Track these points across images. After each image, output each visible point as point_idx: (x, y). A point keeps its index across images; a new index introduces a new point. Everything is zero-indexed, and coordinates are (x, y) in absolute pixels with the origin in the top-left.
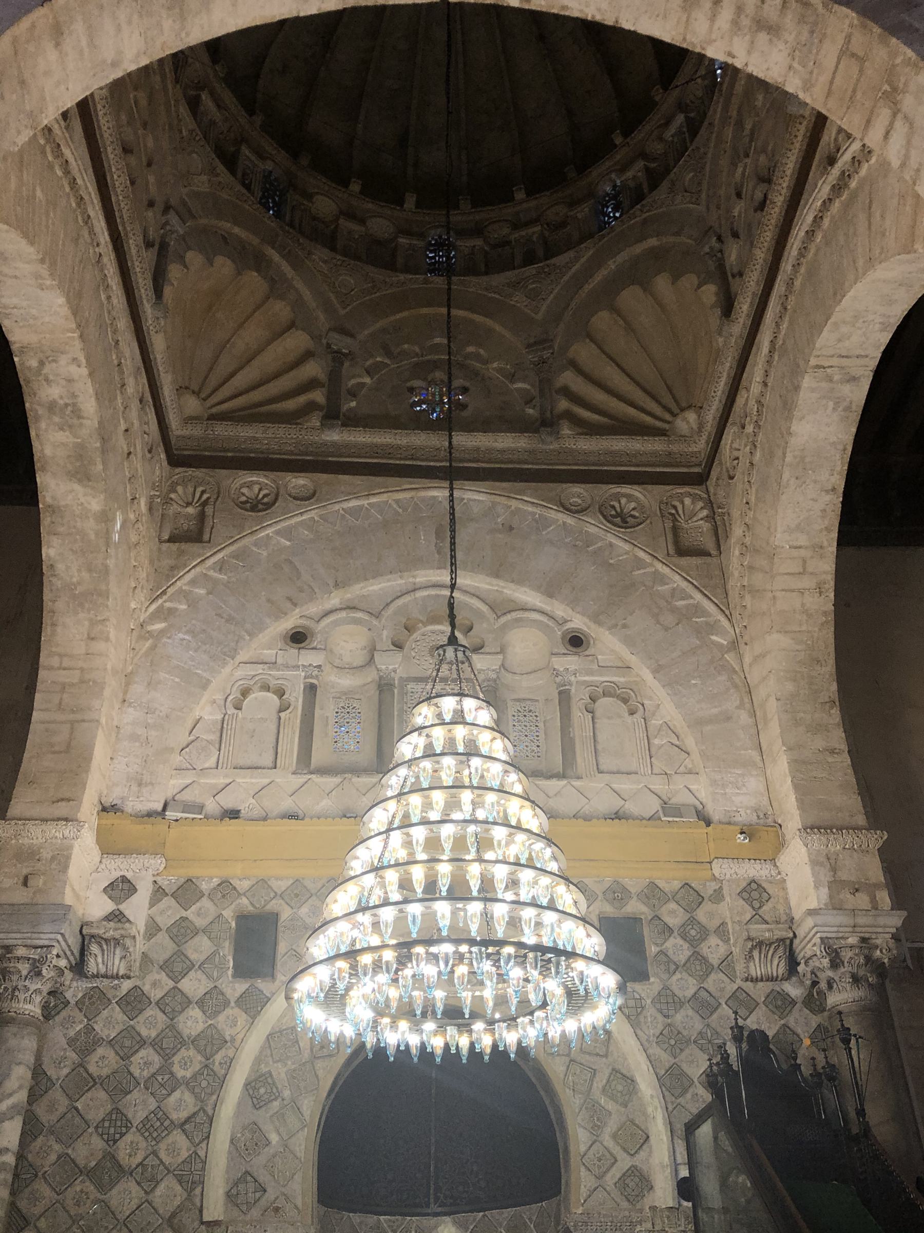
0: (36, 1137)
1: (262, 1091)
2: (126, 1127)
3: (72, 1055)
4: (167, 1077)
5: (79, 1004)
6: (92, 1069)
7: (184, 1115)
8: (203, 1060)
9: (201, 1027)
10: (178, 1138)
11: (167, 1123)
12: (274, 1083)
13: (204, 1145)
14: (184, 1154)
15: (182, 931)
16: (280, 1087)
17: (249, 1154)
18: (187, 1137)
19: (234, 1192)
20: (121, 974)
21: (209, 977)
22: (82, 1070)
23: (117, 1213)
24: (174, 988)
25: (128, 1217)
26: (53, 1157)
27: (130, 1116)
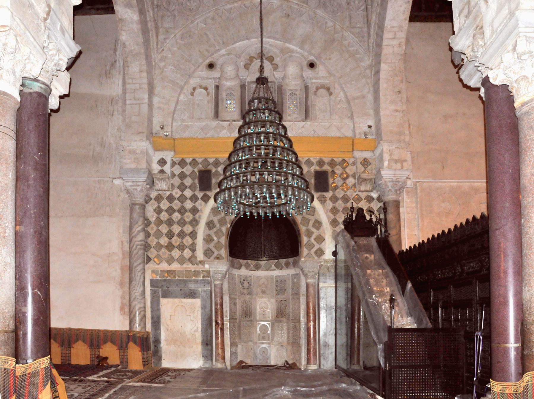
3: (155, 215)
5: (155, 199)
6: (162, 218)
7: (189, 232)
9: (191, 206)
14: (191, 243)
15: (182, 176)
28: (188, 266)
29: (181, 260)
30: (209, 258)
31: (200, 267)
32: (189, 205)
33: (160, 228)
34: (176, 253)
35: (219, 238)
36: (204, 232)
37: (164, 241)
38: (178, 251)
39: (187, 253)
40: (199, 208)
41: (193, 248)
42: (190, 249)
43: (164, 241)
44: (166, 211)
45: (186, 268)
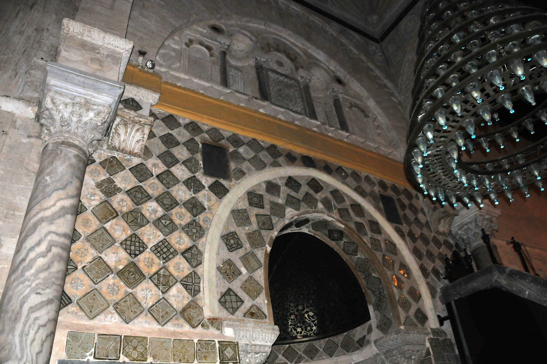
0: (75, 241)
1: (232, 242)
2: (143, 247)
4: (168, 222)
6: (115, 205)
7: (183, 247)
8: (192, 216)
9: (188, 197)
10: (179, 259)
11: (172, 250)
12: (239, 239)
13: (199, 267)
14: (187, 272)
16: (243, 241)
17: (229, 278)
18: (188, 261)
19: (223, 300)
20: (136, 151)
21: (190, 170)
22: (108, 205)
23: (142, 303)
24: (168, 171)
25: (151, 307)
26: (89, 258)
27: (145, 241)
28: (179, 330)
29: (161, 313)
30: (233, 314)
31: (211, 334)
32: (182, 193)
33: (107, 226)
34: (147, 293)
35: (251, 270)
36: (218, 254)
37: (116, 257)
38: (155, 288)
39: (177, 296)
40: (206, 204)
41: (192, 284)
42: (186, 286)
43: (116, 257)
44: (128, 192)
45: (174, 333)
